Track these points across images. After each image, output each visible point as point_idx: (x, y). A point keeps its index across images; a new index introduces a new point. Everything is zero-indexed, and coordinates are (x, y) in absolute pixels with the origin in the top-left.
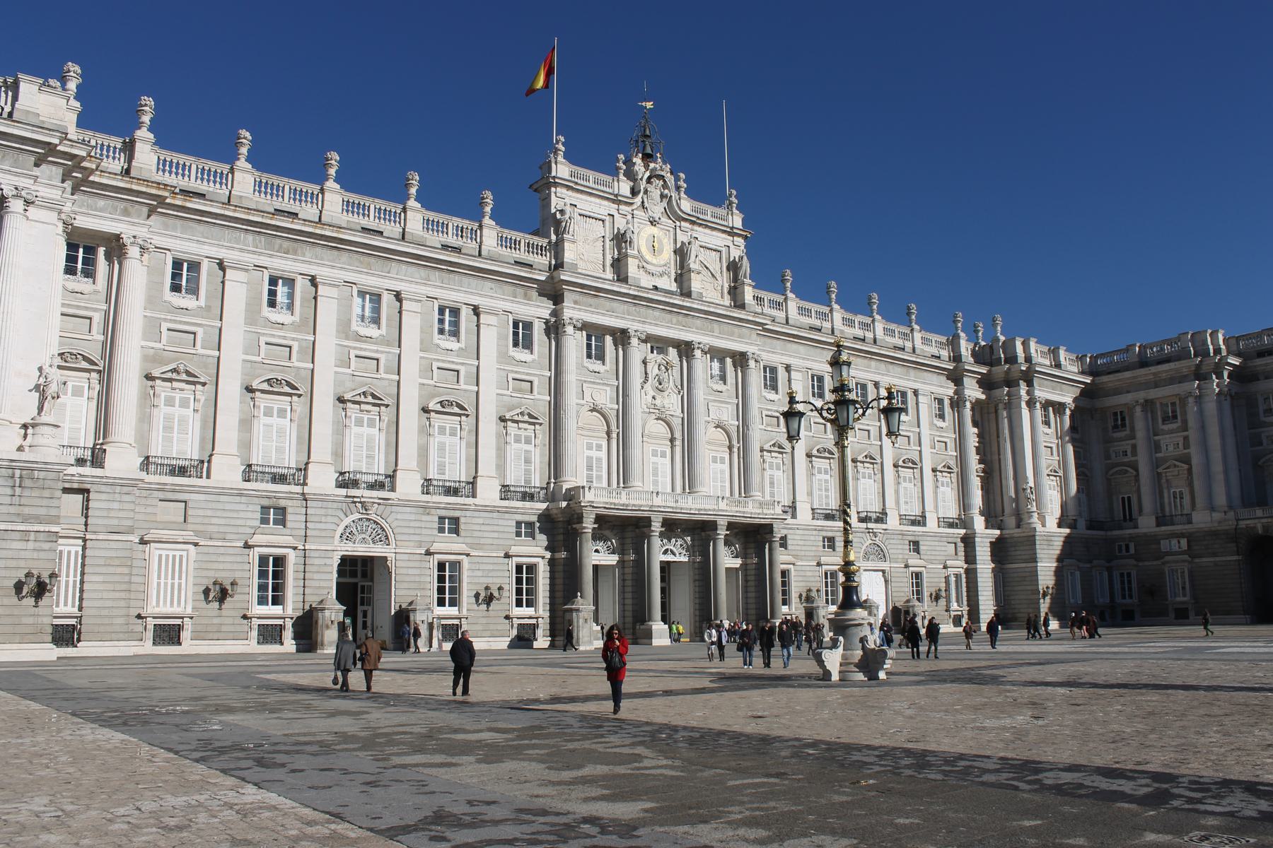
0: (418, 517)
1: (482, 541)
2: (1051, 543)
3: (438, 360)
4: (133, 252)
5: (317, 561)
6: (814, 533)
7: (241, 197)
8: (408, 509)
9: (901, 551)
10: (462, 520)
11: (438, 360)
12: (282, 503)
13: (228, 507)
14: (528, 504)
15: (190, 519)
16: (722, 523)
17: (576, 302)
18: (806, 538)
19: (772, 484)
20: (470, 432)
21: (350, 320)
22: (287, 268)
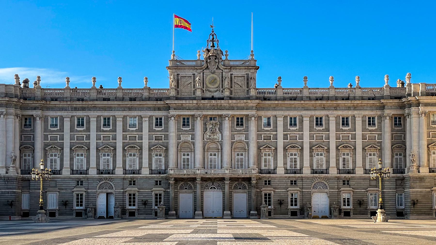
0: (122, 181)
1: (143, 187)
2: (422, 180)
3: (129, 134)
4: (38, 119)
5: (92, 195)
6: (286, 179)
7: (66, 97)
8: (119, 179)
9: (337, 185)
10: (136, 181)
11: (129, 134)
12: (82, 180)
13: (67, 181)
14: (158, 175)
15: (57, 185)
16: (227, 178)
17: (175, 109)
18: (280, 181)
19: (265, 161)
20: (140, 154)
21: (101, 126)
22: (81, 115)
